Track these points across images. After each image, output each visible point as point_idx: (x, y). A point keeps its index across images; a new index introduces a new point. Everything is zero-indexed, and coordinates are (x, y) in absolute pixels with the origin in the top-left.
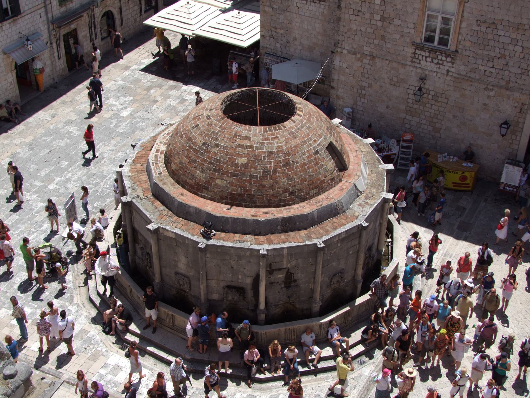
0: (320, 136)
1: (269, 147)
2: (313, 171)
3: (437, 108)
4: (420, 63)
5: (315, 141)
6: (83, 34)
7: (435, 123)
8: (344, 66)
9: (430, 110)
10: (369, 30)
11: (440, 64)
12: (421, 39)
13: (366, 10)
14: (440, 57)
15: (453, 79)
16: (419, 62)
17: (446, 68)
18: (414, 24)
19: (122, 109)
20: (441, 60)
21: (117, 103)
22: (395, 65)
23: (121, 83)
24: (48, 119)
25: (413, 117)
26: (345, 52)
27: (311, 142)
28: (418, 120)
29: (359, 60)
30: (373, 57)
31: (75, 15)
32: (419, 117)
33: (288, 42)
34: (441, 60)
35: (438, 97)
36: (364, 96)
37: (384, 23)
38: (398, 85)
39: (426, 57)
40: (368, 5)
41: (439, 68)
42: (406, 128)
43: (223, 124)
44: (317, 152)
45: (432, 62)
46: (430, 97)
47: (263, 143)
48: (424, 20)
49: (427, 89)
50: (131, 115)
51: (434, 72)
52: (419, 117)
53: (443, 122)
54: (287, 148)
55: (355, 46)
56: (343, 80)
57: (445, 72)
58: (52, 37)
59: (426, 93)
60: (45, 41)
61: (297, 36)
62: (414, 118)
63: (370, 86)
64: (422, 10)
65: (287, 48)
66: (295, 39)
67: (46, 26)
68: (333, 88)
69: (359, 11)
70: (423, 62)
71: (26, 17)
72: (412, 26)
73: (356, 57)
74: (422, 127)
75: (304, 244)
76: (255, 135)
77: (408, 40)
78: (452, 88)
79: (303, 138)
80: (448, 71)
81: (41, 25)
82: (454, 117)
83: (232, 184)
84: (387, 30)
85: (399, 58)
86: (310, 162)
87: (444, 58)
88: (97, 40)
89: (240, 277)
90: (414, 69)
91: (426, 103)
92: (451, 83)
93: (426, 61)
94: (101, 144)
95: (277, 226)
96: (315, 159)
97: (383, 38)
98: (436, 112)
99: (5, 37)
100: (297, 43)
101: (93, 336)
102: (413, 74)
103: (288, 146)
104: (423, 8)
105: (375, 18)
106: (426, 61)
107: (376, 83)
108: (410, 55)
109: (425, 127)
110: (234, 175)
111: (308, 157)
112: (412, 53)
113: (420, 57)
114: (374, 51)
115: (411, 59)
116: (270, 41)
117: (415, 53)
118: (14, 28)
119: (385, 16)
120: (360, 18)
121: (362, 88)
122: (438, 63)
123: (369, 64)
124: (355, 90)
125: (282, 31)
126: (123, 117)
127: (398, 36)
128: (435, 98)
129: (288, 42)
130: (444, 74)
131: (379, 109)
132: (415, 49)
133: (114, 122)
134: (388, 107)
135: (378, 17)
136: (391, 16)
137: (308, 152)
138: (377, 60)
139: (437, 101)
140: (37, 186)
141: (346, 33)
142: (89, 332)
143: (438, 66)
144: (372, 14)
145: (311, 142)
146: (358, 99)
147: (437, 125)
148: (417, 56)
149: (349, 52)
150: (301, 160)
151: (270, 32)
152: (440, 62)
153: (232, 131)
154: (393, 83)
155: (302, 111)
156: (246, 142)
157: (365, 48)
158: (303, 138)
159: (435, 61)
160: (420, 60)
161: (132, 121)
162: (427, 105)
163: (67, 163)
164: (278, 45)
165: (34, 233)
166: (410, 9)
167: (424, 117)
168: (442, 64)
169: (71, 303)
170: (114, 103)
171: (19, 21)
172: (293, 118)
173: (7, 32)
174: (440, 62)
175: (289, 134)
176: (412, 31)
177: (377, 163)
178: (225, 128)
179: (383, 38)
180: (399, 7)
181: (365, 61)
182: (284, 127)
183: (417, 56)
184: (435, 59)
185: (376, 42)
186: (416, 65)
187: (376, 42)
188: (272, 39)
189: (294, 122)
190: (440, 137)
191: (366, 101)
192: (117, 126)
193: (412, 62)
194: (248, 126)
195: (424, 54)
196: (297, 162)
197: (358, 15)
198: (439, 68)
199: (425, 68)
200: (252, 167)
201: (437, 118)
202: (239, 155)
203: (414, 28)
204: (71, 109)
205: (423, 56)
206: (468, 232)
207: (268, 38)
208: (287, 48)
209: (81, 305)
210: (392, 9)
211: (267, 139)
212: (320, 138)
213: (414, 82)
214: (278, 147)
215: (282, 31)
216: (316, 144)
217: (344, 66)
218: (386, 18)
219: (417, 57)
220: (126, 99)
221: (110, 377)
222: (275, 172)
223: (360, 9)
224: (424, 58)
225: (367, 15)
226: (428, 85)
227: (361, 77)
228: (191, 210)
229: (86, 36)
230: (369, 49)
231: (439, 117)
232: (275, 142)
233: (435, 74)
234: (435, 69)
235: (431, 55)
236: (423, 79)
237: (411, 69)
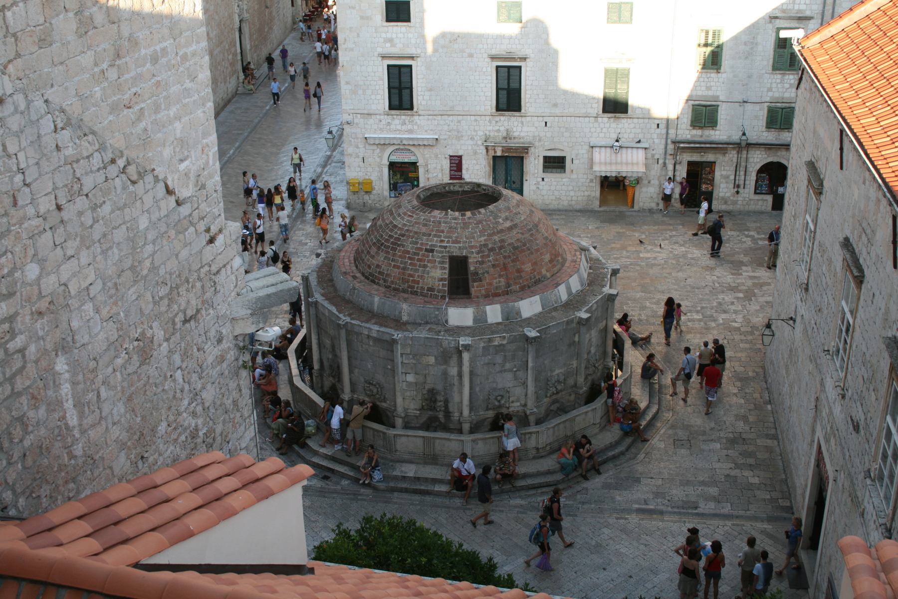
5: (442, 241)
6: (724, 173)
31: (721, 148)
58: (668, 157)
60: (656, 157)
67: (663, 141)
71: (635, 121)
81: (655, 136)
86: (415, 254)
88: (746, 190)
96: (423, 255)
99: (598, 130)
103: (411, 228)
111: (417, 249)
118: (614, 125)
137: (422, 244)
171: (624, 121)
173: (602, 125)
229: (727, 177)
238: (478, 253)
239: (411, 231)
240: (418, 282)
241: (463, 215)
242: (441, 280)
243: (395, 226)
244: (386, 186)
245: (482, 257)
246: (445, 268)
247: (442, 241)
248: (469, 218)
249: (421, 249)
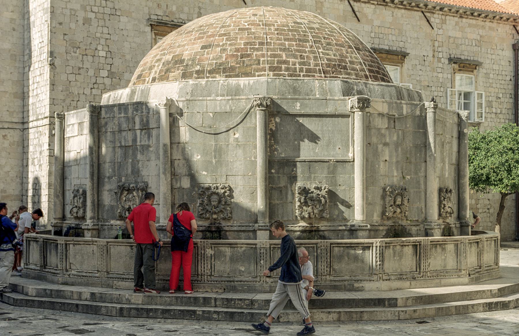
13: (89, 67)
40: (90, 58)
69: (80, 69)
105: (101, 75)
120: (82, 76)
135: (104, 73)
136: (119, 70)
141: (64, 101)
180: (128, 57)
197: (79, 74)
210: (121, 61)
223: (81, 66)
225: (91, 73)
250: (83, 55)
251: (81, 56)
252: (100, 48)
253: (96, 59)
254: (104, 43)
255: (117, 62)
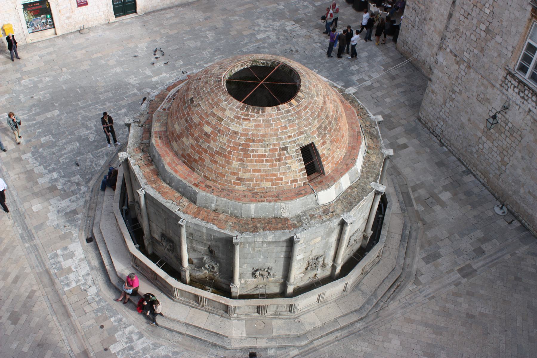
0: (301, 133)
1: (236, 127)
2: (270, 166)
3: (510, 142)
4: (507, 90)
5: (290, 137)
7: (505, 156)
8: (445, 64)
9: (504, 141)
10: (473, 37)
11: (525, 99)
12: (515, 66)
13: (475, 16)
14: (527, 92)
15: (532, 120)
16: (507, 88)
17: (530, 106)
18: (513, 47)
19: (262, 31)
20: (527, 96)
21: (262, 25)
22: (485, 82)
23: (281, 7)
24: (201, 20)
25: (487, 140)
26: (448, 50)
27: (283, 136)
28: (491, 145)
29: (457, 63)
30: (469, 67)
32: (493, 143)
33: (425, 20)
34: (527, 96)
35: (514, 132)
36: (452, 100)
37: (488, 35)
38: (483, 103)
39: (515, 87)
40: (478, 10)
41: (523, 103)
42: (479, 148)
43: (216, 87)
44: (285, 149)
45: (519, 94)
46: (507, 128)
47: (232, 120)
48: (523, 47)
49: (507, 119)
50: (264, 39)
51: (517, 105)
52: (493, 143)
53: (511, 158)
54: (253, 135)
55: (457, 49)
56: (441, 77)
57: (527, 110)
59: (505, 123)
61: (434, 17)
62: (488, 142)
63: (460, 92)
64: (524, 36)
65: (423, 26)
66: (431, 19)
68: (430, 80)
69: (469, 14)
70: (510, 90)
72: (510, 49)
73: (455, 59)
74: (492, 153)
75: (223, 231)
76: (231, 109)
77: (503, 61)
78: (528, 129)
79: (277, 130)
80: (530, 111)
82: (523, 158)
83: (192, 147)
84: (488, 43)
85: (491, 76)
87: (530, 95)
89: (171, 232)
90: (501, 94)
91: (502, 133)
92: (530, 124)
93: (514, 90)
94: (220, 56)
95: (211, 203)
96: (280, 155)
97: (482, 50)
98: (508, 145)
100: (432, 23)
101: (77, 219)
102: (499, 98)
103: (255, 132)
104: (525, 34)
105: (481, 27)
106: (514, 90)
107: (465, 93)
108: (501, 77)
109: (495, 155)
110: (197, 140)
112: (503, 77)
113: (509, 84)
114: (471, 59)
115: (500, 82)
116: (412, 12)
117: (506, 78)
119: (490, 28)
121: (454, 92)
122: (523, 98)
123: (464, 71)
124: (448, 90)
125: (423, 7)
126: (257, 38)
127: (496, 55)
128: (512, 131)
129: (425, 20)
130: (525, 112)
131: (462, 119)
132: (507, 74)
133: (246, 40)
134: (469, 120)
137: (274, 145)
138: (472, 70)
139: (511, 135)
140: (145, 74)
142: (78, 214)
143: (522, 100)
144: (479, 22)
145: (283, 136)
146: (448, 100)
147: (506, 159)
148: (507, 81)
149: (451, 52)
150: (261, 151)
151: (414, 4)
152: (526, 98)
153: (216, 97)
154: (480, 99)
155: (298, 101)
156: (219, 114)
157: (465, 54)
158: (277, 130)
159: (522, 95)
160: (508, 87)
161: (260, 44)
162: (503, 135)
163: (182, 63)
164: (417, 19)
165: (112, 112)
166: (513, 30)
167: (497, 145)
168: (527, 100)
169: (86, 184)
170: (260, 23)
172: (280, 106)
174: (526, 98)
175: (263, 121)
176: (509, 54)
177: (371, 179)
178: (213, 92)
179: (482, 50)
180: (505, 24)
181: (462, 66)
182: (263, 112)
183: (507, 81)
184: (522, 92)
185: (476, 51)
186: (504, 91)
187: (476, 51)
188: (414, 11)
189: (279, 109)
190: (505, 171)
191: (453, 106)
192: (246, 44)
193: (501, 85)
194: (231, 98)
195: (513, 82)
196: (256, 151)
197: (467, 18)
198: (523, 103)
199: (511, 97)
200: (213, 139)
201: (507, 152)
202: (208, 123)
203: (512, 52)
204: (224, 17)
205: (512, 84)
206: (466, 279)
207: (411, 10)
208: (423, 26)
209: (91, 189)
210: (498, 24)
211: (239, 118)
212: (299, 136)
213: (497, 105)
214: (245, 130)
215: (423, 7)
216: (289, 141)
217: (445, 64)
218: (490, 30)
219: (506, 83)
220: (272, 24)
221: (61, 259)
222: (230, 152)
223: (470, 13)
224: (513, 86)
225: (475, 21)
226: (509, 115)
227: (454, 80)
228: (157, 156)
230: (468, 56)
231: (509, 151)
232: (245, 123)
233: (517, 108)
234: (519, 103)
235: (519, 87)
236: (505, 108)
237: (499, 92)
238: (318, 136)
239: (257, 135)
240: (282, 179)
241: (291, 105)
242: (301, 170)
243: (236, 133)
244: (25, 26)
245: (322, 138)
246: (301, 160)
247: (290, 137)
248: (297, 106)
249: (276, 150)
250: (474, 5)
251: (472, 5)
252: (487, 5)
253: (482, 13)
254: (491, 3)
255: (495, 23)
